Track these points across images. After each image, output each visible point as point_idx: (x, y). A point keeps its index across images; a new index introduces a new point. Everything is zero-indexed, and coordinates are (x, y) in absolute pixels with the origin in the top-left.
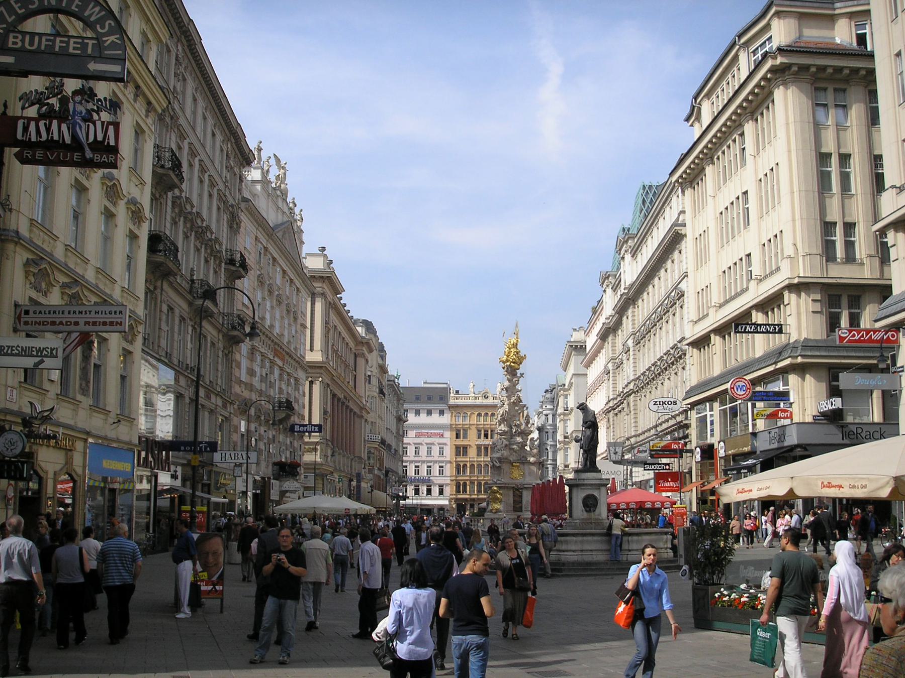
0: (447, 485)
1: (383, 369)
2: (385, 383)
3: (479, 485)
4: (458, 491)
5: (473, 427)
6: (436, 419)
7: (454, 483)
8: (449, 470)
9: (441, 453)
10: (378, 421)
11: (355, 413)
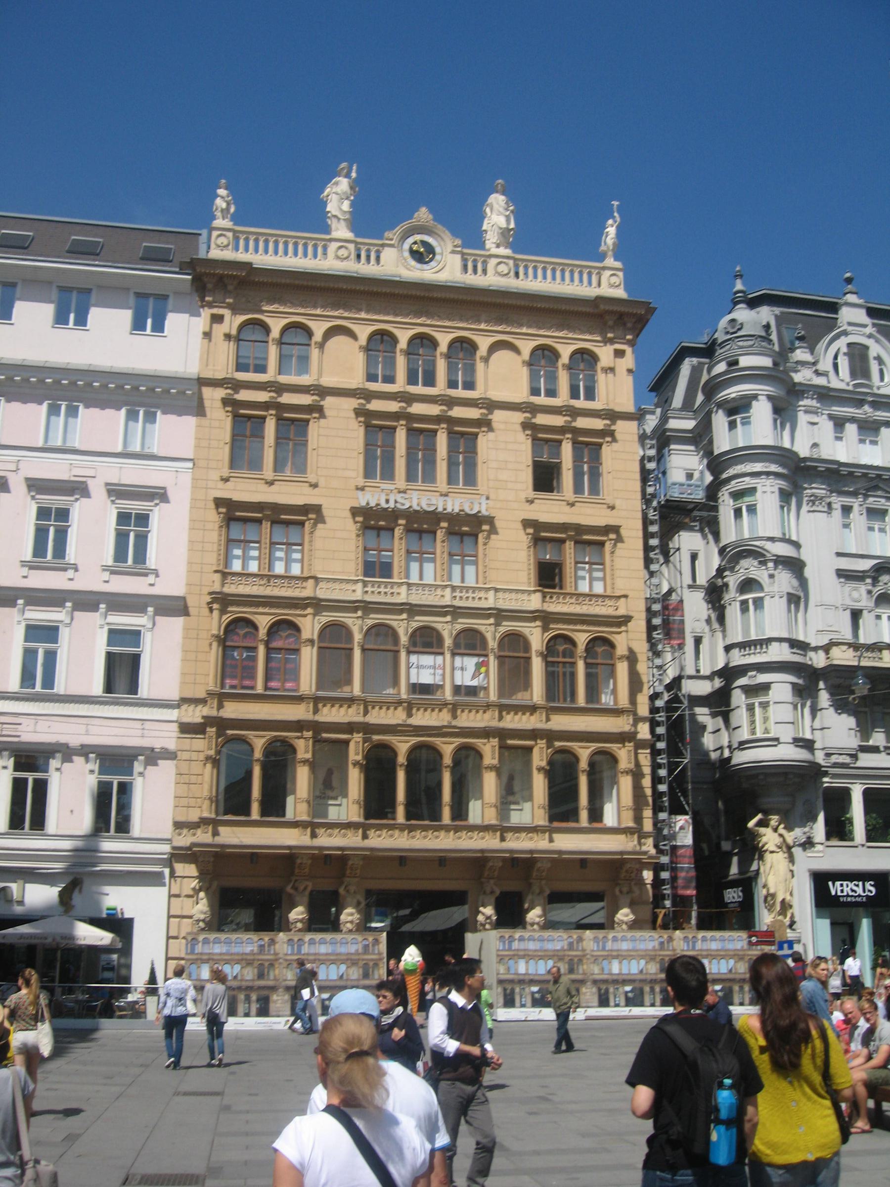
0: (153, 757)
3: (379, 766)
4: (233, 801)
5: (339, 409)
6: (108, 339)
7: (203, 745)
8: (171, 660)
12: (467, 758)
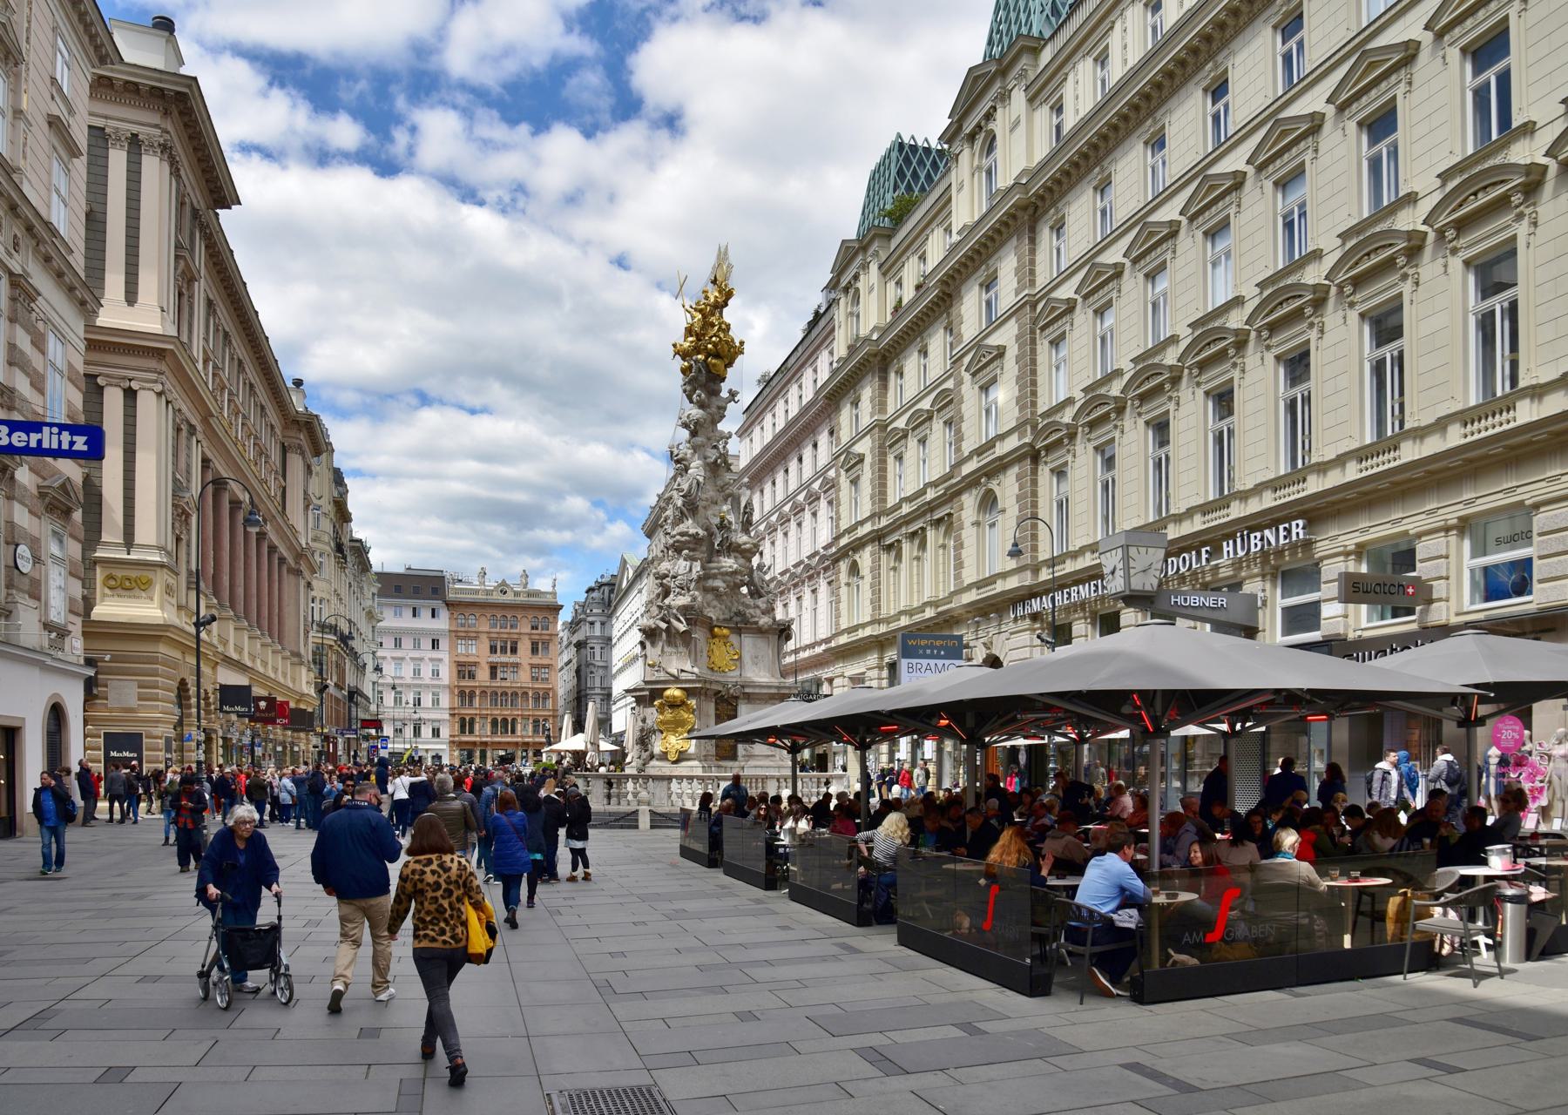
1: (343, 515)
2: (345, 541)
6: (425, 622)
9: (436, 673)
10: (334, 600)
11: (282, 560)
12: (514, 720)
